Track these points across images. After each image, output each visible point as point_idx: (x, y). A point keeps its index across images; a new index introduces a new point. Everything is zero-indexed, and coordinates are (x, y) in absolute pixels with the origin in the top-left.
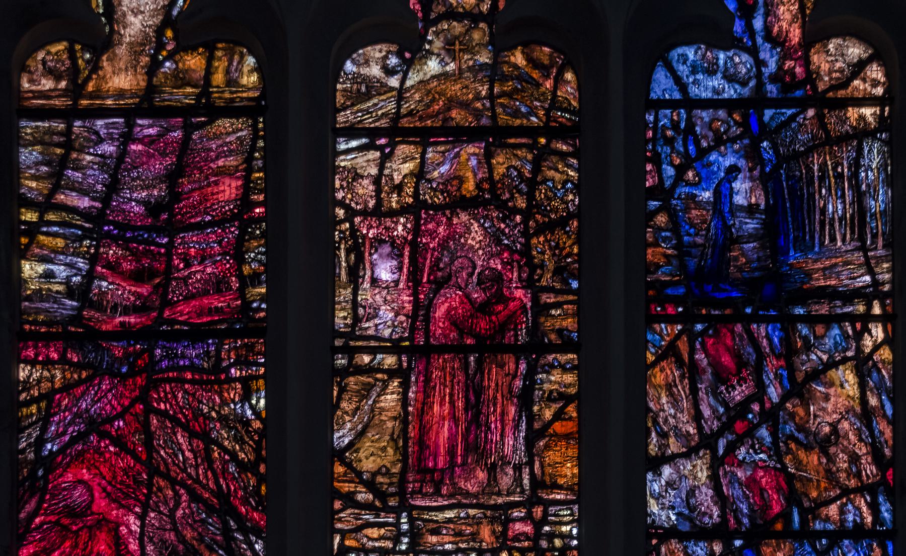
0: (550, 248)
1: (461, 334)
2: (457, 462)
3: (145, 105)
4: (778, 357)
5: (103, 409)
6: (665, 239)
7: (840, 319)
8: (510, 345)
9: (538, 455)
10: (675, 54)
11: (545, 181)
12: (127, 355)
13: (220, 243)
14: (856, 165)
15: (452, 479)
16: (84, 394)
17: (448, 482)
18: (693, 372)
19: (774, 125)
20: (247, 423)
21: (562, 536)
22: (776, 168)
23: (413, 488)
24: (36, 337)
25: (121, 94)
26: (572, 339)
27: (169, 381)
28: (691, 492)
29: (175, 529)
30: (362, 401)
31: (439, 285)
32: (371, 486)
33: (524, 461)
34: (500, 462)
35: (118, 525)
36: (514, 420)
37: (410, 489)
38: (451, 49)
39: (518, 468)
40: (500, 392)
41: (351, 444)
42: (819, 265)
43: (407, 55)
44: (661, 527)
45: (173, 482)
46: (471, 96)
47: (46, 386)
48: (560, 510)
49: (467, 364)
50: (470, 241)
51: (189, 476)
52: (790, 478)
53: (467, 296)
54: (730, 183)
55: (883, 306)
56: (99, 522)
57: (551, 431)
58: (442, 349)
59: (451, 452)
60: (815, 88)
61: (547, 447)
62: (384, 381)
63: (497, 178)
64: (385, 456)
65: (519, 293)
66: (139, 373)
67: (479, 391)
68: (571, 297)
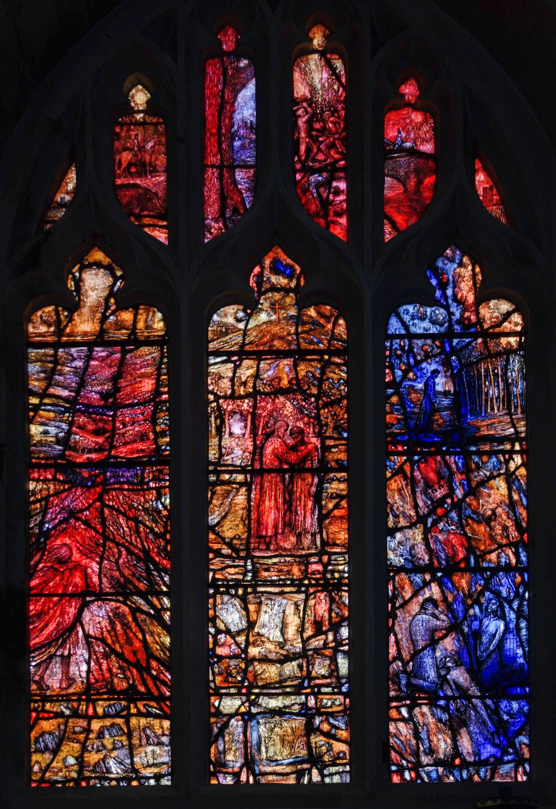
0: (331, 415)
1: (281, 462)
3: (99, 340)
4: (461, 474)
5: (78, 505)
6: (397, 410)
7: (497, 453)
9: (325, 528)
10: (402, 309)
11: (328, 379)
12: (91, 476)
13: (143, 414)
14: (505, 369)
15: (276, 541)
16: (66, 497)
18: (413, 482)
19: (459, 347)
20: (159, 512)
21: (339, 572)
22: (460, 371)
24: (39, 466)
25: (85, 334)
26: (344, 465)
27: (115, 489)
28: (412, 547)
29: (119, 569)
31: (268, 436)
32: (230, 545)
35: (86, 568)
36: (311, 509)
38: (273, 307)
39: (314, 535)
41: (218, 523)
42: (484, 423)
43: (249, 311)
44: (395, 566)
45: (117, 544)
46: (285, 333)
47: (45, 493)
49: (284, 480)
50: (285, 412)
51: (127, 541)
52: (469, 539)
53: (284, 442)
55: (521, 445)
56: (75, 566)
57: (332, 515)
58: (270, 471)
59: (276, 527)
60: (482, 327)
61: (330, 523)
62: (237, 489)
63: (300, 377)
65: (314, 440)
66: (98, 486)
67: (291, 493)
68: (343, 442)
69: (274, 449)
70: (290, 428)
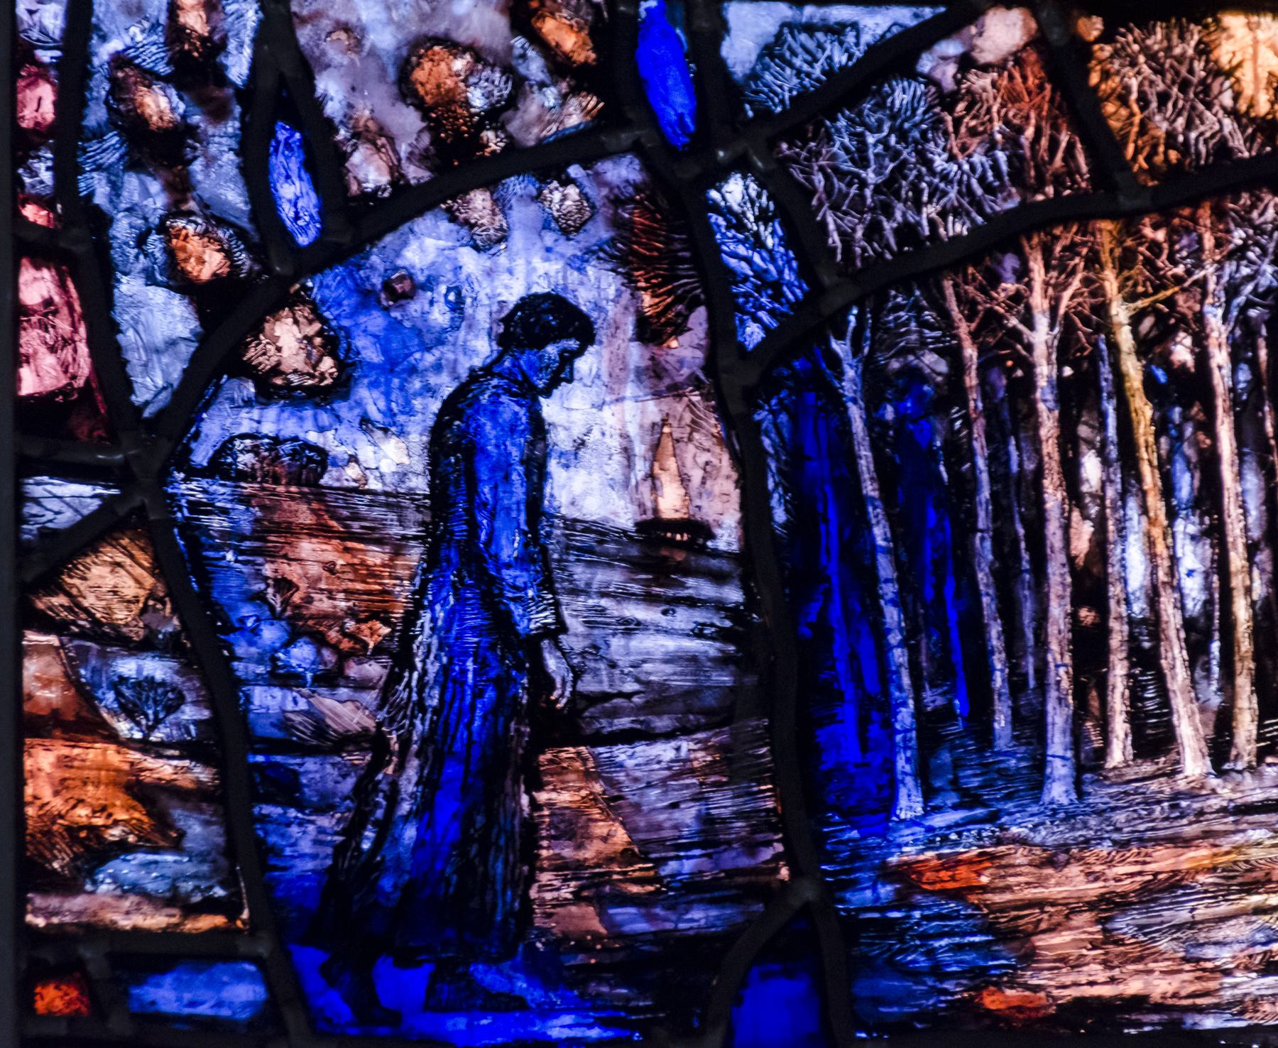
54: (530, 395)
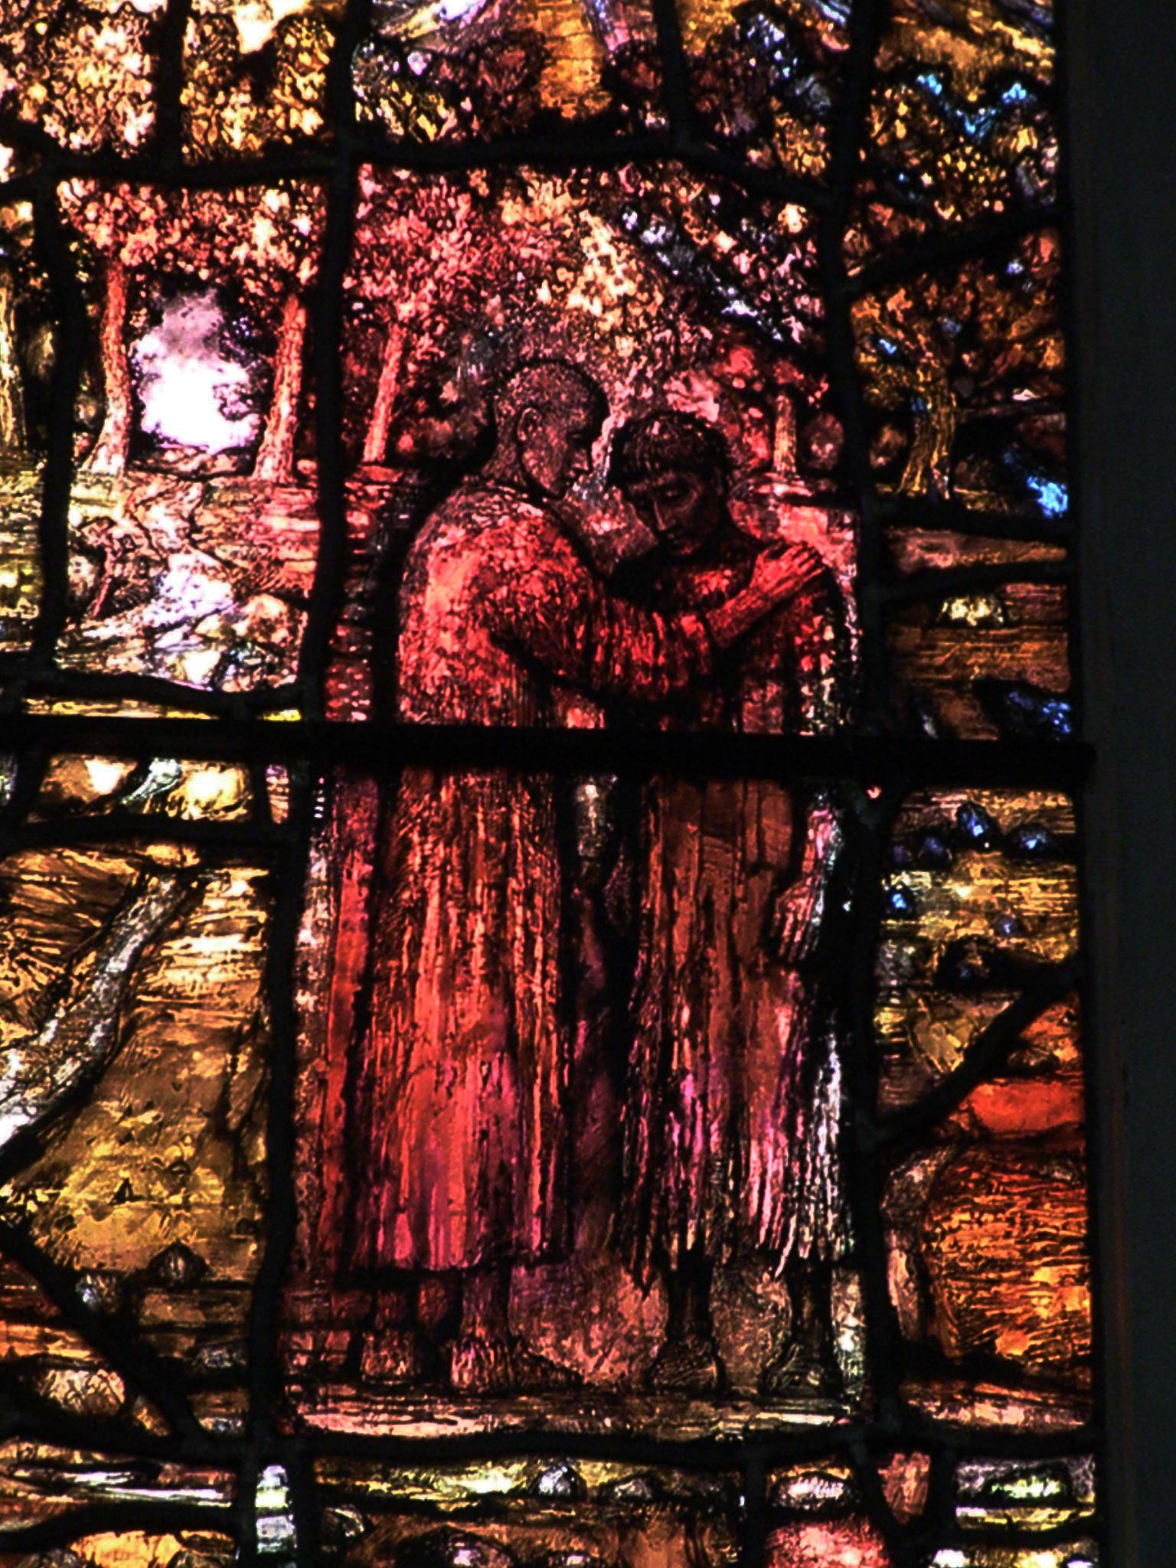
0: (937, 335)
2: (524, 1244)
8: (761, 738)
11: (908, 70)
15: (498, 1315)
17: (480, 1332)
23: (314, 1354)
30: (81, 956)
33: (839, 1247)
34: (726, 1252)
37: (303, 1360)
40: (721, 941)
48: (1011, 1478)
49: (570, 813)
50: (575, 299)
62: (180, 874)
64: (186, 1205)
68: (1039, 552)
69: (480, 586)
70: (615, 420)
